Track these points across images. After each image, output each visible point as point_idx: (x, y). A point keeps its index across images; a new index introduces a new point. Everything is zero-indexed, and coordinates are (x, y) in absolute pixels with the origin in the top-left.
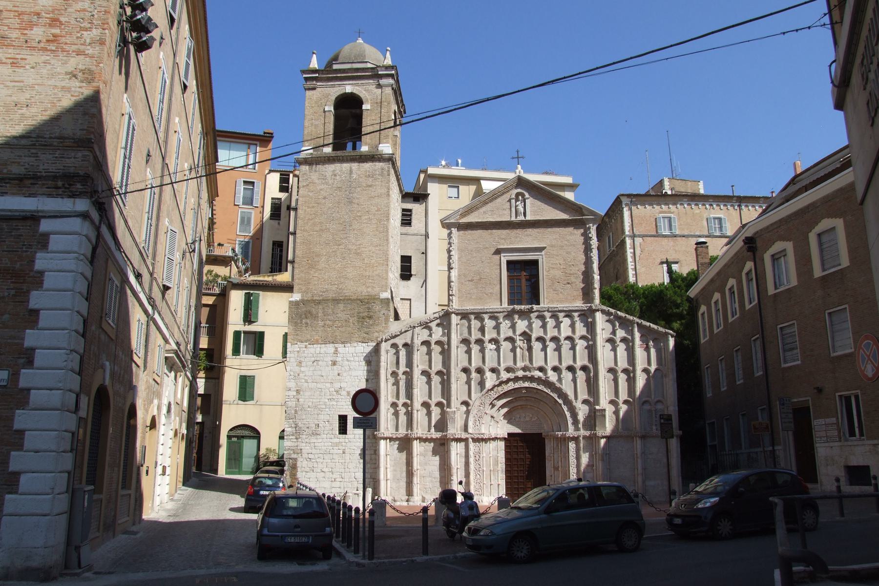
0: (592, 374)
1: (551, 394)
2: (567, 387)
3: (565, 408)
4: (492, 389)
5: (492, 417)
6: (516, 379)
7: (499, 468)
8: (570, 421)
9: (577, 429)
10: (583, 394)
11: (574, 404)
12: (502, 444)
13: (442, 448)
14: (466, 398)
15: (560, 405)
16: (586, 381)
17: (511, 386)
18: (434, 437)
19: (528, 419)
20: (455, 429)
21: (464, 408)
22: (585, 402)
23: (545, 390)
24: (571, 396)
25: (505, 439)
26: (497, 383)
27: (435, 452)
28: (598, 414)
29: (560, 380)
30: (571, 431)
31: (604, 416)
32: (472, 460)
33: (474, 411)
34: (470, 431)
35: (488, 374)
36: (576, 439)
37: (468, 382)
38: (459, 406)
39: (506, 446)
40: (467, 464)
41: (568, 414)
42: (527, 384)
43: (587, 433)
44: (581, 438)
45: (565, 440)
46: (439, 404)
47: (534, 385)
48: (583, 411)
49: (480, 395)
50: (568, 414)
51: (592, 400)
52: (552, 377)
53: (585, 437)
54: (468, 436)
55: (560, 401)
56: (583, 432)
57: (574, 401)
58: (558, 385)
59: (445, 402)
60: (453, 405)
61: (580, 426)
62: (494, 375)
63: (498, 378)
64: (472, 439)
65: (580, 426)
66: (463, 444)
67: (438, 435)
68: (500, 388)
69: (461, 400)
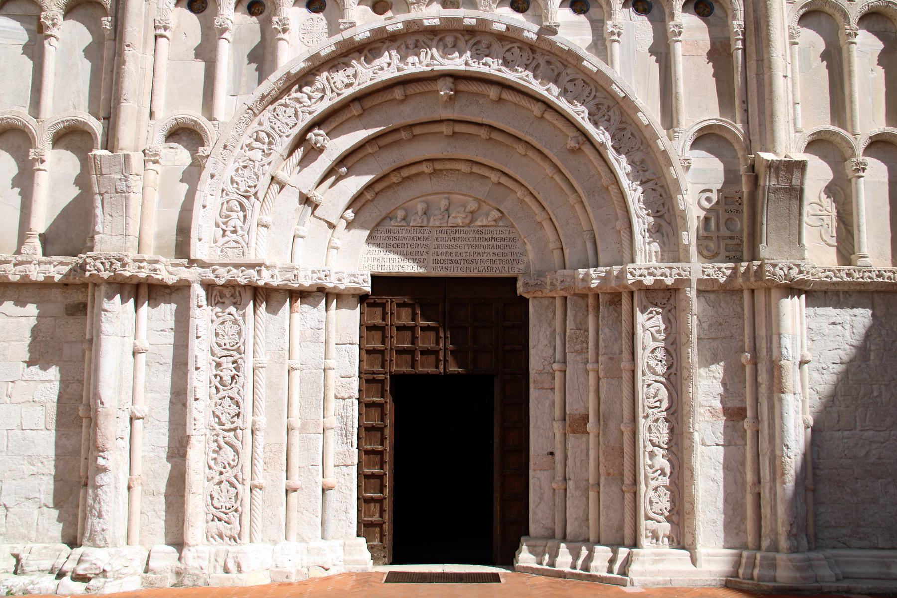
0: (737, 24)
1: (563, 104)
2: (629, 69)
3: (622, 166)
4: (304, 78)
5: (306, 200)
6: (415, 37)
7: (333, 421)
8: (642, 221)
9: (672, 250)
10: (700, 104)
11: (663, 141)
12: (347, 322)
13: (72, 324)
14: (193, 112)
15: (598, 150)
16: (712, 55)
17: (388, 66)
18: (36, 274)
19: (459, 218)
20: (133, 236)
21: (181, 156)
22: (707, 138)
23: (536, 86)
24: (649, 111)
25: (362, 298)
26: (326, 45)
27: (41, 352)
28: (769, 182)
29: (601, 44)
30: (647, 262)
31: (797, 194)
32: (200, 381)
33: (222, 168)
34: (198, 250)
35: (293, 15)
36: (665, 297)
37: (206, 53)
38: (157, 141)
39: (367, 329)
40: (180, 397)
41: (634, 194)
42: (457, 62)
43: (720, 271)
44: (692, 292)
45: (617, 302)
46: (71, 136)
47: (492, 67)
48: (698, 179)
49: (252, 99)
50: (634, 194)
51: (738, 128)
52: (572, 31)
53: (707, 289)
54: (186, 273)
55: (601, 135)
56: (696, 268)
57: (661, 132)
58: (592, 62)
59: (97, 126)
60: (126, 135)
61: (689, 237)
62: (320, 21)
63: (333, 29)
64: (209, 286)
65: (689, 237)
66: (167, 311)
67: (56, 269)
68: (340, 77)
69: (166, 117)
